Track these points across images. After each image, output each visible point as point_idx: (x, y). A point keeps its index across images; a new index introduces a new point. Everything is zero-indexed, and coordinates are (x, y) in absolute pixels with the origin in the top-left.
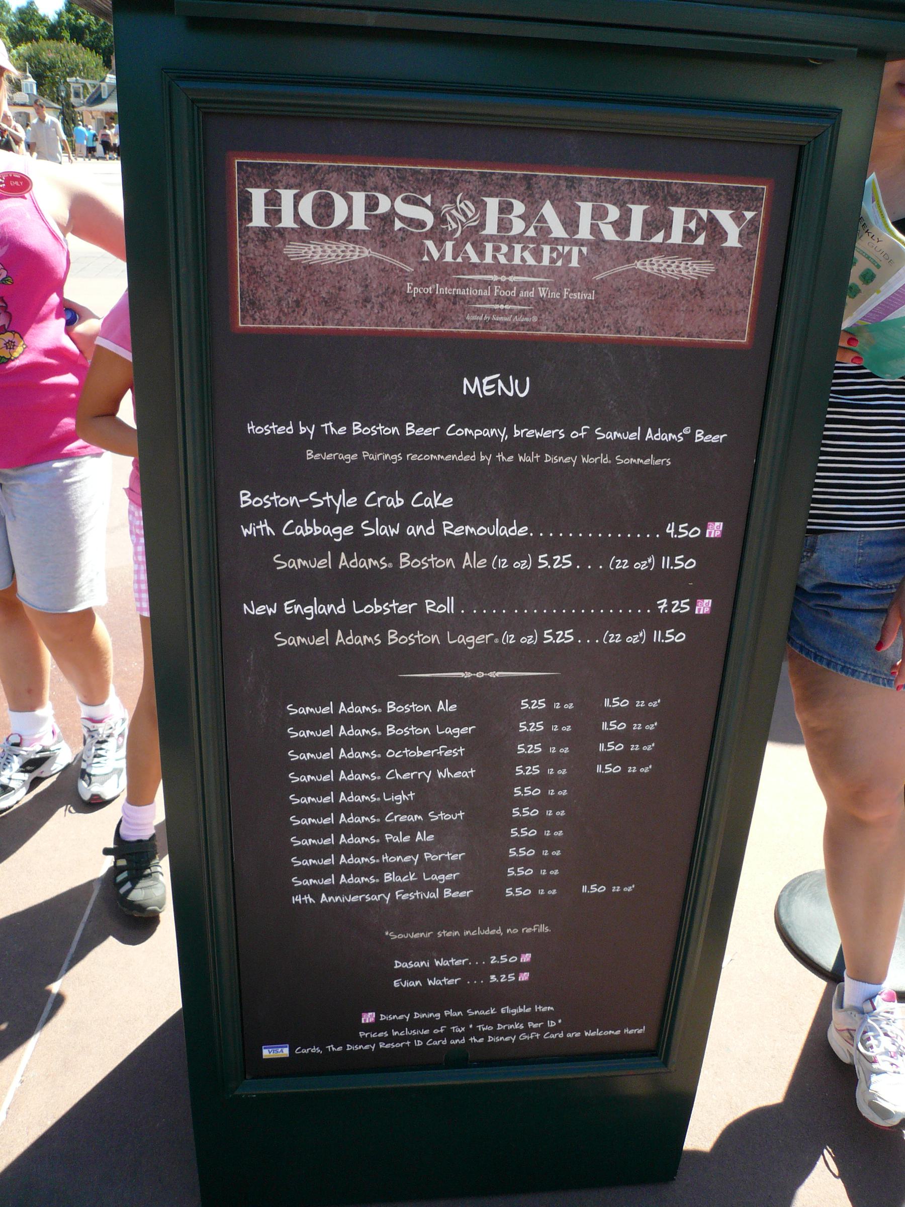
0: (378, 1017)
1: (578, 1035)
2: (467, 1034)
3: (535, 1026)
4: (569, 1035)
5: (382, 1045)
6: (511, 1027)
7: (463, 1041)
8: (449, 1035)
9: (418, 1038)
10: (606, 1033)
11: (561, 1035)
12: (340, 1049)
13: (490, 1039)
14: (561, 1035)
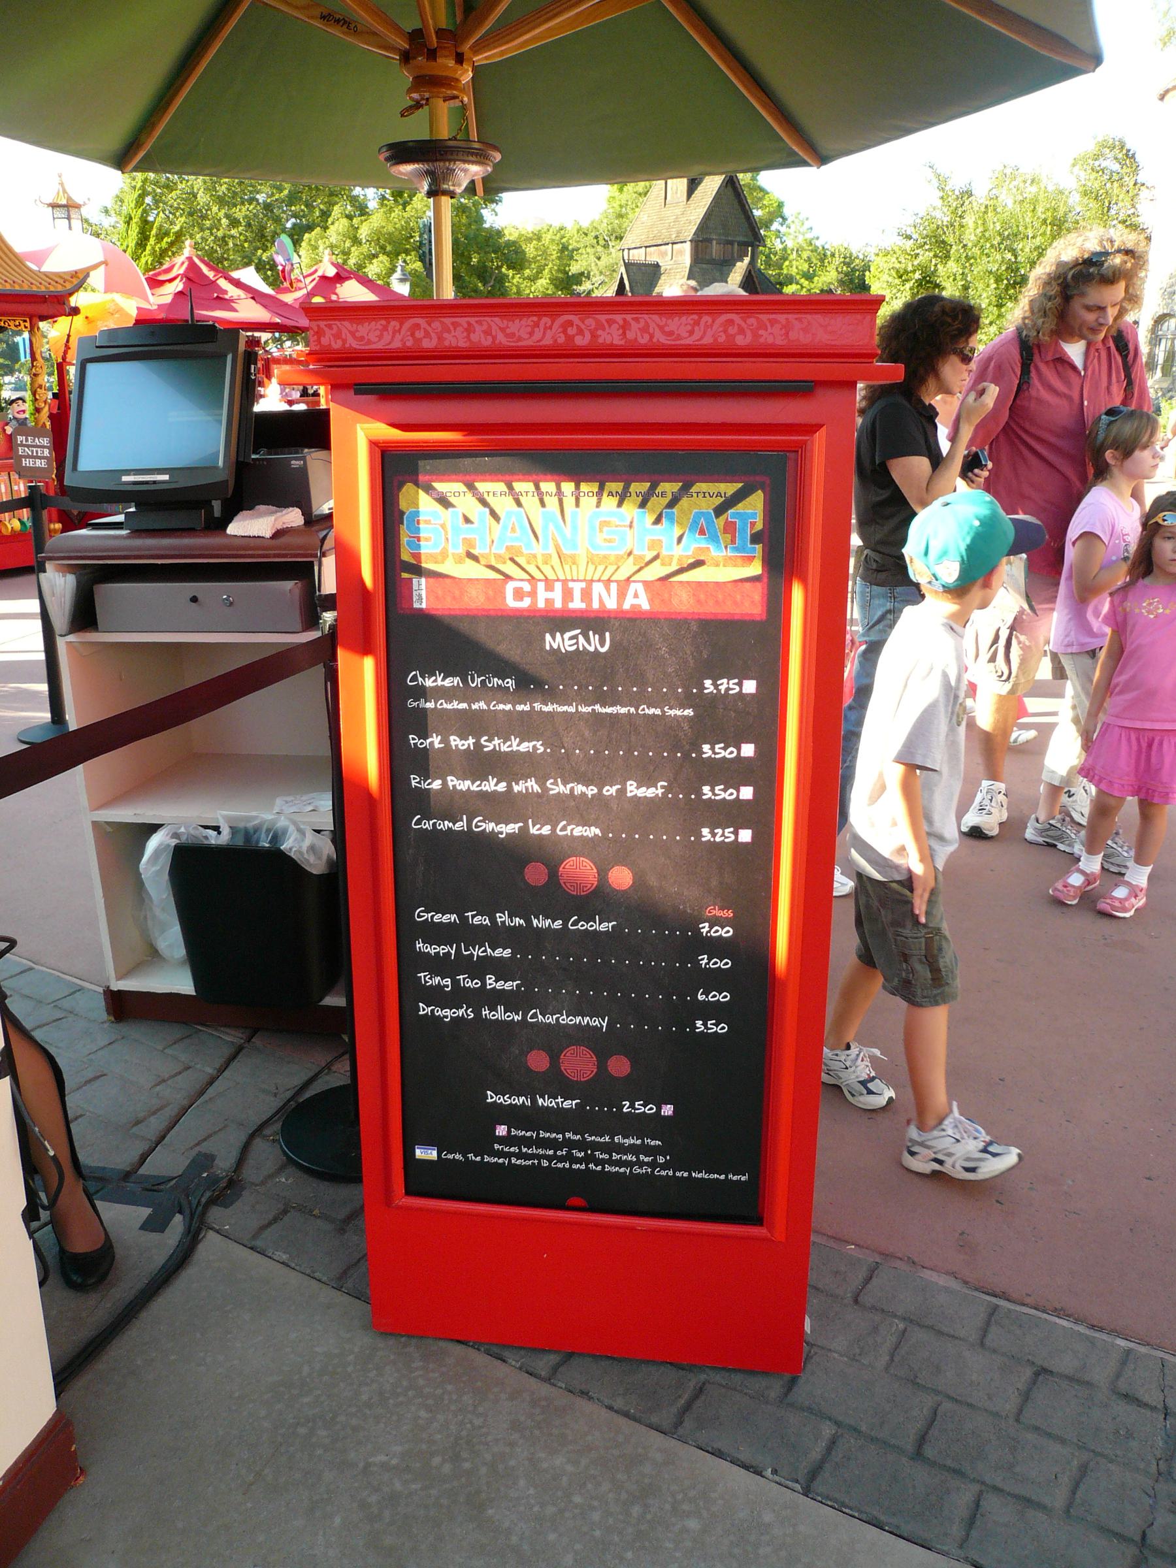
0: (509, 1131)
1: (686, 1174)
2: (587, 1159)
3: (646, 1159)
4: (678, 1174)
5: (513, 1160)
6: (624, 1158)
7: (583, 1167)
8: (570, 1158)
9: (544, 1158)
10: (712, 1176)
11: (671, 1173)
12: (478, 1159)
13: (608, 1168)
14: (671, 1173)
